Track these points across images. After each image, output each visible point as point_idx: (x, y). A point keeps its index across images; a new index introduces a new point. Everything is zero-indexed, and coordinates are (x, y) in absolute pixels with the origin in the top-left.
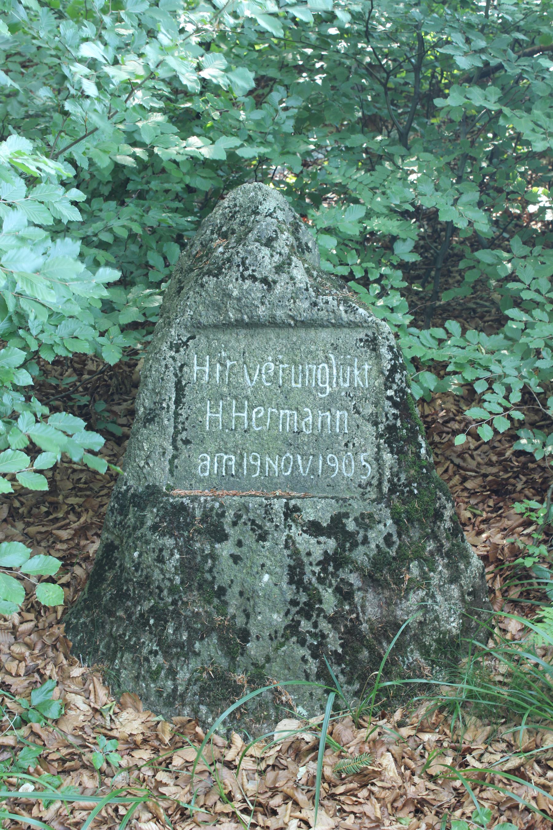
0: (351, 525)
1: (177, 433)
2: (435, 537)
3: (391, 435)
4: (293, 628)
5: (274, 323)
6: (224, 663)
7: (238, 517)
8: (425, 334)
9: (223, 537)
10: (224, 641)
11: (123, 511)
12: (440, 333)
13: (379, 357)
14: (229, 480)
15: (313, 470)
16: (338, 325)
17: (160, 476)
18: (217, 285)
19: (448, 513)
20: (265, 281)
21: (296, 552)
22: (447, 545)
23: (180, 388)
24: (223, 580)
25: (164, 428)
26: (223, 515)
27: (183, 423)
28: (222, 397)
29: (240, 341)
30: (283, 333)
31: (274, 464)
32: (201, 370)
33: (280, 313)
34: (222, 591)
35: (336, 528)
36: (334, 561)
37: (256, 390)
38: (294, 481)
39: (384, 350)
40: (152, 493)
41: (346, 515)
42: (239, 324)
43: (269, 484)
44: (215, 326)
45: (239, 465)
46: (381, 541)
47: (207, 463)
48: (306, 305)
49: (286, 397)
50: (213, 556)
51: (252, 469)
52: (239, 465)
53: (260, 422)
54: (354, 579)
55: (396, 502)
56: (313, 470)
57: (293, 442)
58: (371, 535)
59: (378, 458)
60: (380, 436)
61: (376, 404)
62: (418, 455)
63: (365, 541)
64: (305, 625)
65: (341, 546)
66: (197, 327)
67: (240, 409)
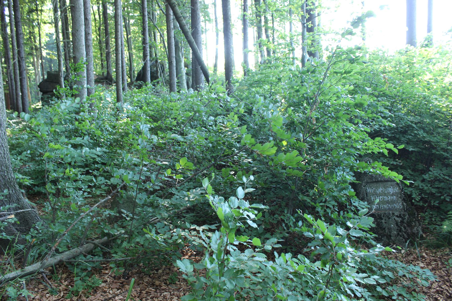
2: (414, 218)
3: (404, 200)
4: (398, 234)
5: (381, 181)
6: (388, 241)
9: (382, 219)
10: (387, 237)
15: (392, 207)
21: (396, 221)
23: (366, 194)
24: (384, 226)
29: (375, 185)
31: (385, 206)
32: (369, 190)
34: (384, 229)
36: (402, 222)
37: (380, 193)
42: (375, 182)
43: (385, 210)
45: (379, 207)
50: (382, 222)
51: (382, 207)
52: (379, 207)
53: (381, 199)
54: (405, 225)
56: (392, 207)
57: (388, 202)
59: (403, 204)
64: (400, 233)
66: (367, 183)
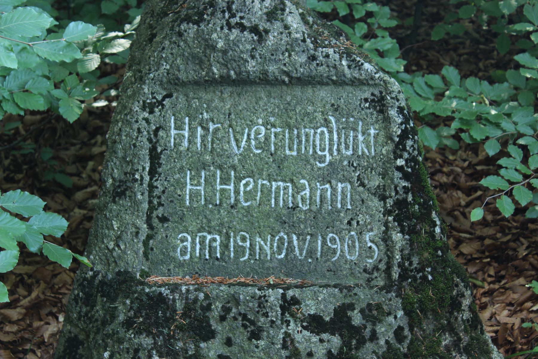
0: (357, 319)
1: (152, 208)
2: (452, 330)
3: (400, 212)
5: (264, 80)
7: (226, 310)
8: (419, 80)
9: (210, 335)
11: (89, 301)
12: (435, 80)
13: (387, 120)
14: (212, 265)
15: (311, 253)
16: (340, 82)
17: (133, 260)
18: (199, 34)
19: (466, 302)
20: (254, 30)
22: (465, 339)
23: (155, 157)
25: (137, 204)
26: (208, 308)
27: (159, 197)
28: (205, 166)
29: (225, 100)
30: (276, 91)
31: (266, 245)
32: (179, 134)
33: (272, 68)
35: (339, 323)
37: (244, 158)
38: (289, 265)
39: (393, 113)
40: (124, 282)
41: (351, 307)
42: (224, 81)
43: (260, 267)
44: (196, 83)
45: (225, 246)
46: (391, 335)
47: (187, 245)
48: (303, 59)
49: (279, 167)
53: (249, 196)
55: (408, 291)
56: (311, 253)
57: (287, 219)
58: (380, 329)
59: (386, 239)
60: (387, 212)
61: (384, 175)
62: (432, 234)
63: (374, 337)
65: (346, 343)
66: (173, 84)
67: (225, 180)
